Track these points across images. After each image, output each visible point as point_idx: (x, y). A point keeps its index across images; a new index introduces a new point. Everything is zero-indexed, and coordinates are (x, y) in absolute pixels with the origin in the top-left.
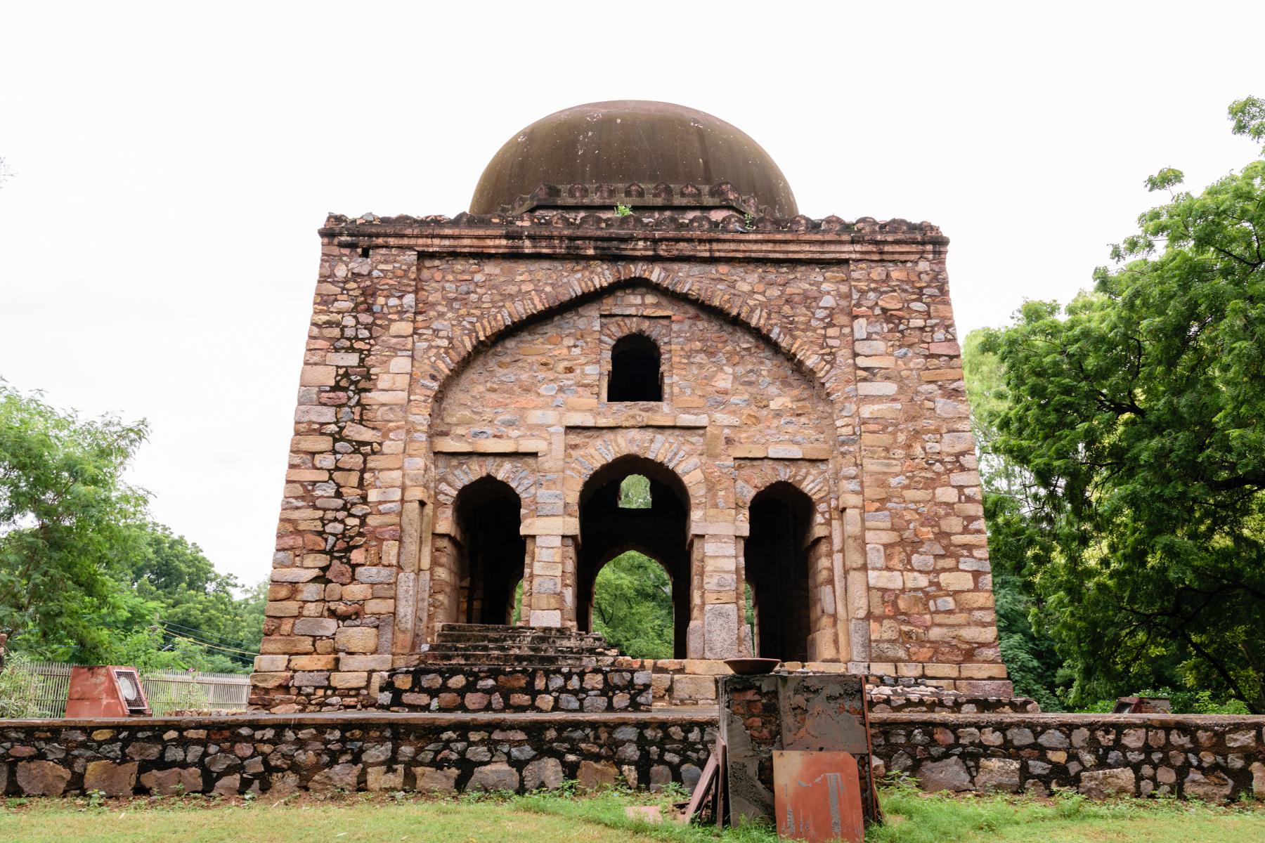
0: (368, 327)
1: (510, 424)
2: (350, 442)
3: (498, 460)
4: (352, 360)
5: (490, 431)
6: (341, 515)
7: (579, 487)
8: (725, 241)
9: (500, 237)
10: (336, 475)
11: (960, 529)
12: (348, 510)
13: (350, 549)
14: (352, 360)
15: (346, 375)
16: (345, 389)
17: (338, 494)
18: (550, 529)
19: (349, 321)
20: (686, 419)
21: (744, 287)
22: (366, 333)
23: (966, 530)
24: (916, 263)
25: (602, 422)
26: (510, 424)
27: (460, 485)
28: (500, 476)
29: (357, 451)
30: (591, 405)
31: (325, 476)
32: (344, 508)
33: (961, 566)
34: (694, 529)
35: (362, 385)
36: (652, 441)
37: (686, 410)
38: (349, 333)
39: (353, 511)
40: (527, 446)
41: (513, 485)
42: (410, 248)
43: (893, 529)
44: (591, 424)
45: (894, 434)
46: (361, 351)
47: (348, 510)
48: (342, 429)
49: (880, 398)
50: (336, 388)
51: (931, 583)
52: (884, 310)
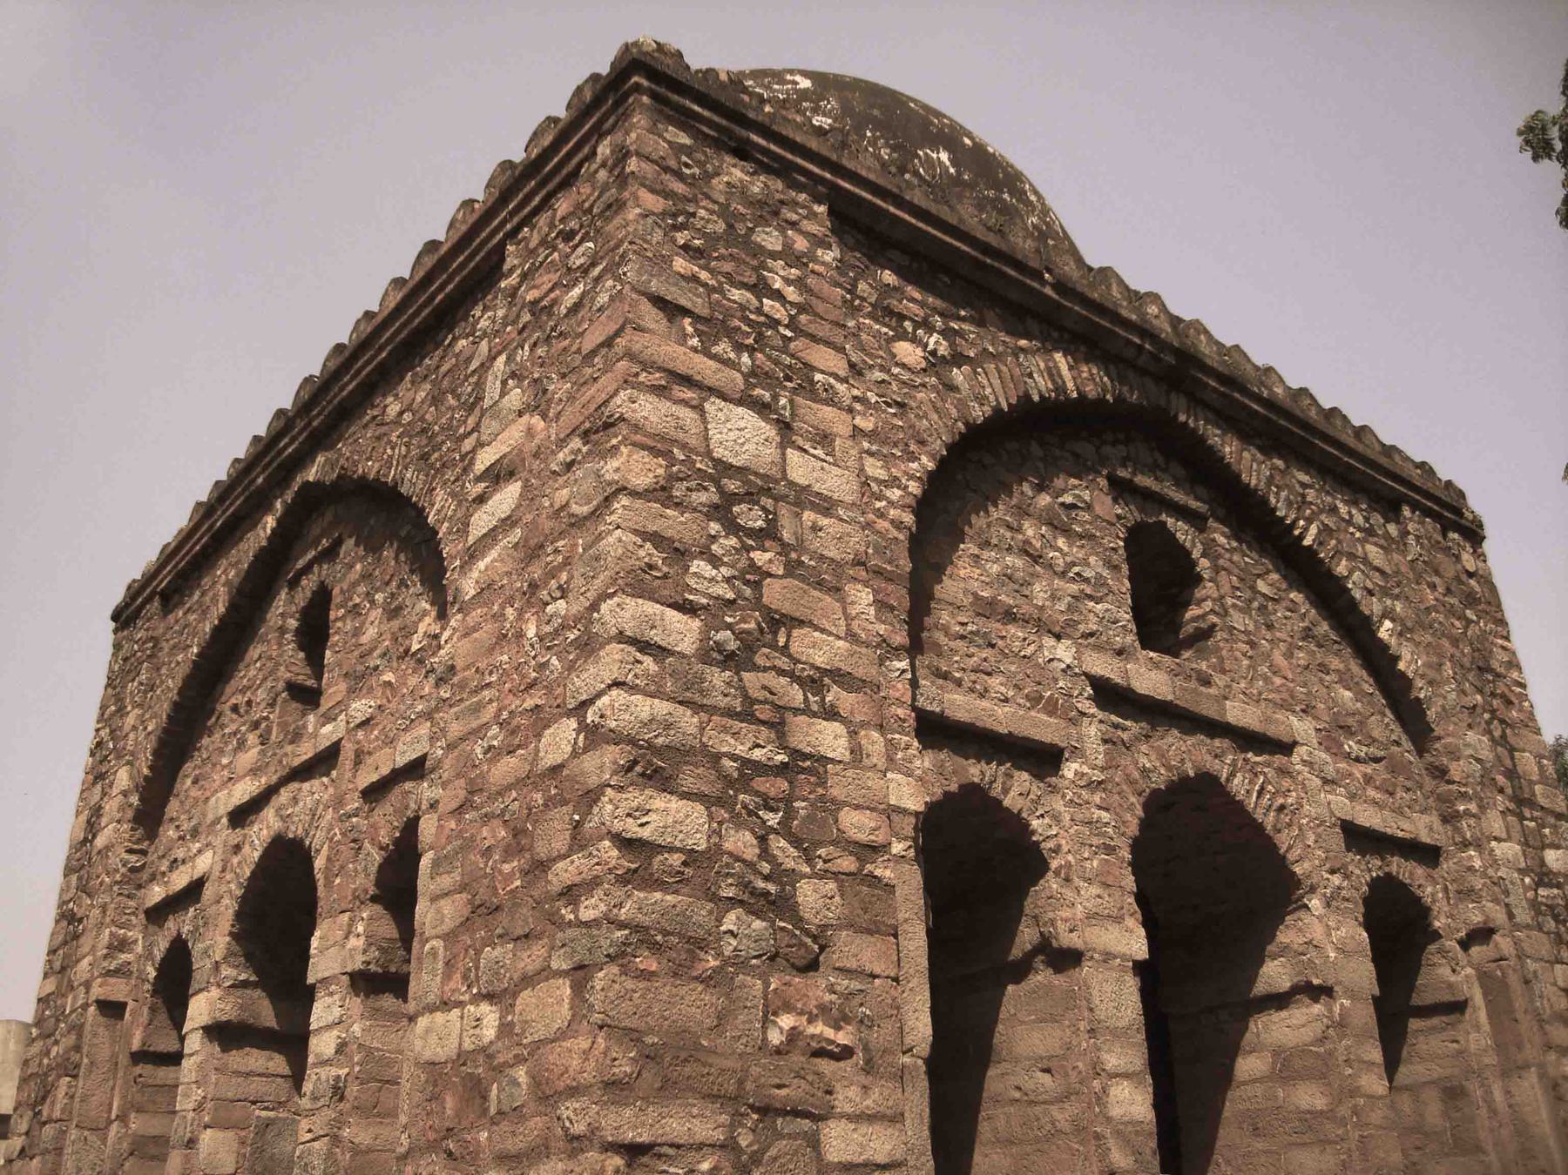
1: (195, 833)
5: (180, 853)
11: (560, 843)
21: (393, 409)
23: (579, 841)
24: (594, 153)
27: (158, 958)
33: (554, 965)
34: (310, 980)
36: (295, 800)
42: (154, 593)
43: (463, 887)
45: (499, 617)
49: (491, 536)
51: (505, 1029)
52: (535, 303)
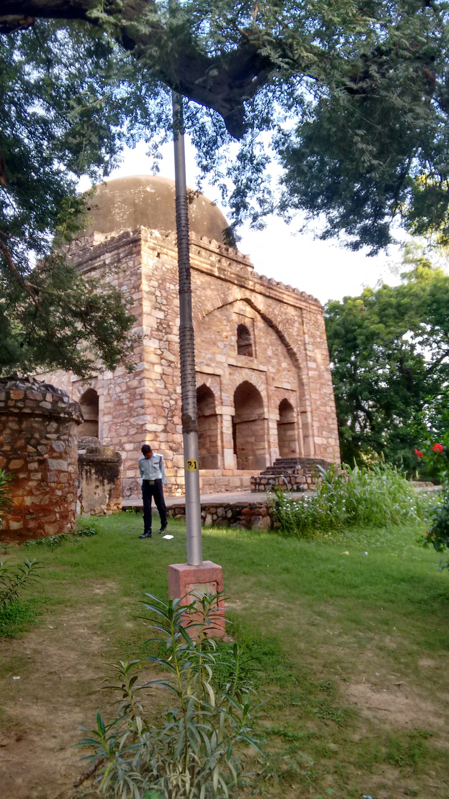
0: (166, 298)
2: (166, 360)
3: (207, 376)
4: (161, 315)
6: (168, 398)
7: (233, 393)
8: (276, 290)
9: (207, 264)
10: (164, 376)
12: (170, 396)
13: (173, 416)
14: (161, 315)
15: (161, 324)
16: (161, 331)
17: (166, 387)
18: (226, 411)
19: (158, 293)
20: (262, 368)
22: (165, 302)
25: (239, 365)
26: (210, 359)
28: (208, 385)
29: (169, 366)
30: (234, 357)
31: (159, 378)
32: (169, 395)
35: (168, 330)
37: (261, 363)
38: (159, 300)
39: (172, 397)
40: (218, 371)
41: (212, 389)
44: (235, 364)
46: (164, 311)
47: (170, 396)
48: (163, 352)
50: (158, 330)
